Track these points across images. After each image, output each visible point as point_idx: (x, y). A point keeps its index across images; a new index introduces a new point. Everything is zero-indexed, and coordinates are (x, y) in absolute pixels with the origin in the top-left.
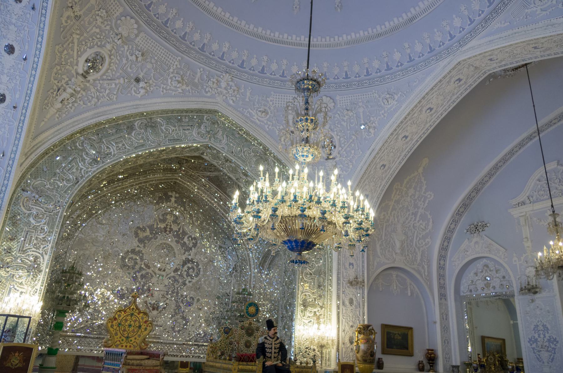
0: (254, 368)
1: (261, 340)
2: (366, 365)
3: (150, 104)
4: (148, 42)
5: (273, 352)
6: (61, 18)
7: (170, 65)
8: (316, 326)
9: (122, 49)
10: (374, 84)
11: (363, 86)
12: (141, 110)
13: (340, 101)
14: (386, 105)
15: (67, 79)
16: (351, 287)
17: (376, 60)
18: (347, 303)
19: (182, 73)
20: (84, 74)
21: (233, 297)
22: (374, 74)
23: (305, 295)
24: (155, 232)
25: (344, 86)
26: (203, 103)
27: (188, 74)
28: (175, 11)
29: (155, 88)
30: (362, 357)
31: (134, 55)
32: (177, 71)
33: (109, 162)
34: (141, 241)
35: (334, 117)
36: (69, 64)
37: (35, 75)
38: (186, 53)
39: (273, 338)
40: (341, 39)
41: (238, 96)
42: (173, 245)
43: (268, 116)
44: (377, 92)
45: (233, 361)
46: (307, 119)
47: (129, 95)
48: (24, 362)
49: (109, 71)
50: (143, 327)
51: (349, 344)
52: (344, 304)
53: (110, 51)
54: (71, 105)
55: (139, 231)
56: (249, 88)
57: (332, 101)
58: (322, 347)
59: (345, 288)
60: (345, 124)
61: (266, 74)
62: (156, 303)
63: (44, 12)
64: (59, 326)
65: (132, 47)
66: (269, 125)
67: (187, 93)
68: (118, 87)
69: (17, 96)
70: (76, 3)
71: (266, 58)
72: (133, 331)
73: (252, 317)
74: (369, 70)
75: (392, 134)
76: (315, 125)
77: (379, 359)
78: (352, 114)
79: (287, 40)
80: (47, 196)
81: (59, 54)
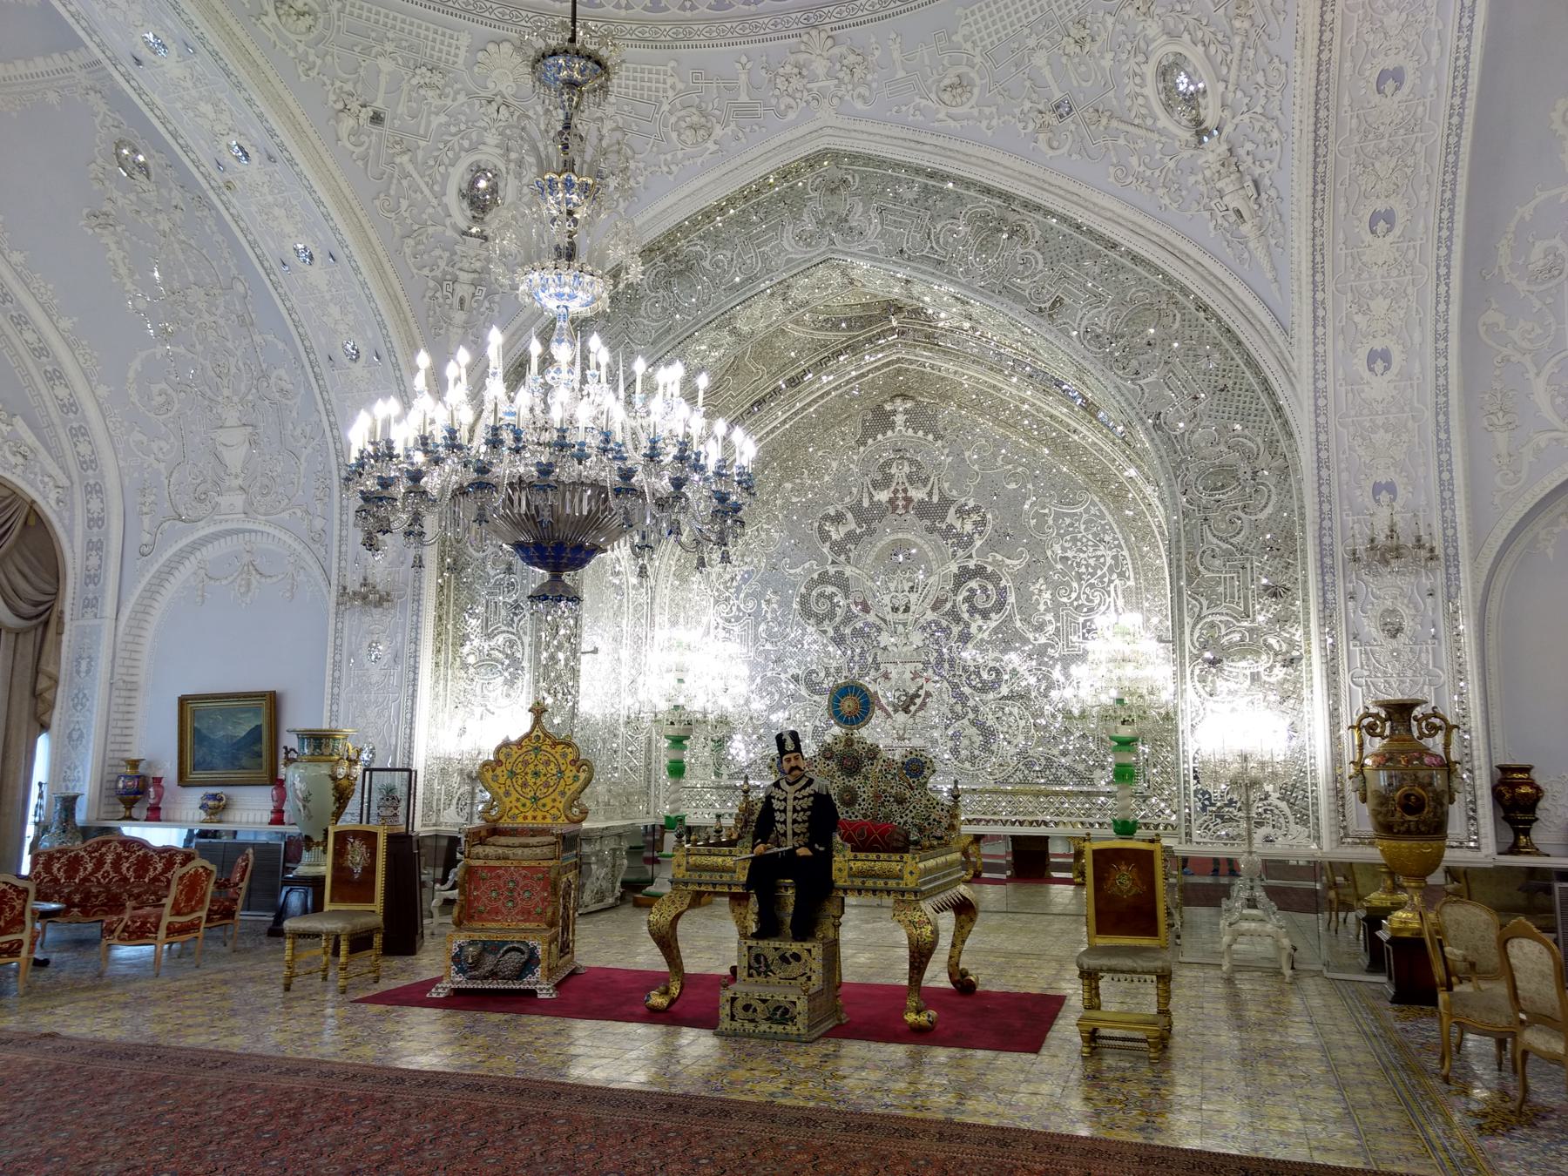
0: (729, 862)
5: (789, 821)
7: (657, 97)
18: (1371, 629)
23: (1212, 625)
24: (868, 517)
34: (839, 548)
36: (429, 223)
38: (681, 40)
43: (976, 91)
54: (487, 304)
55: (828, 527)
56: (893, 36)
66: (991, 117)
69: (370, 335)
72: (547, 785)
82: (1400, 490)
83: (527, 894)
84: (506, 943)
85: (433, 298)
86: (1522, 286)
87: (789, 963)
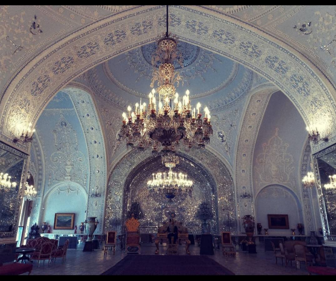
0: (165, 235)
50: (137, 224)
82: (246, 188)
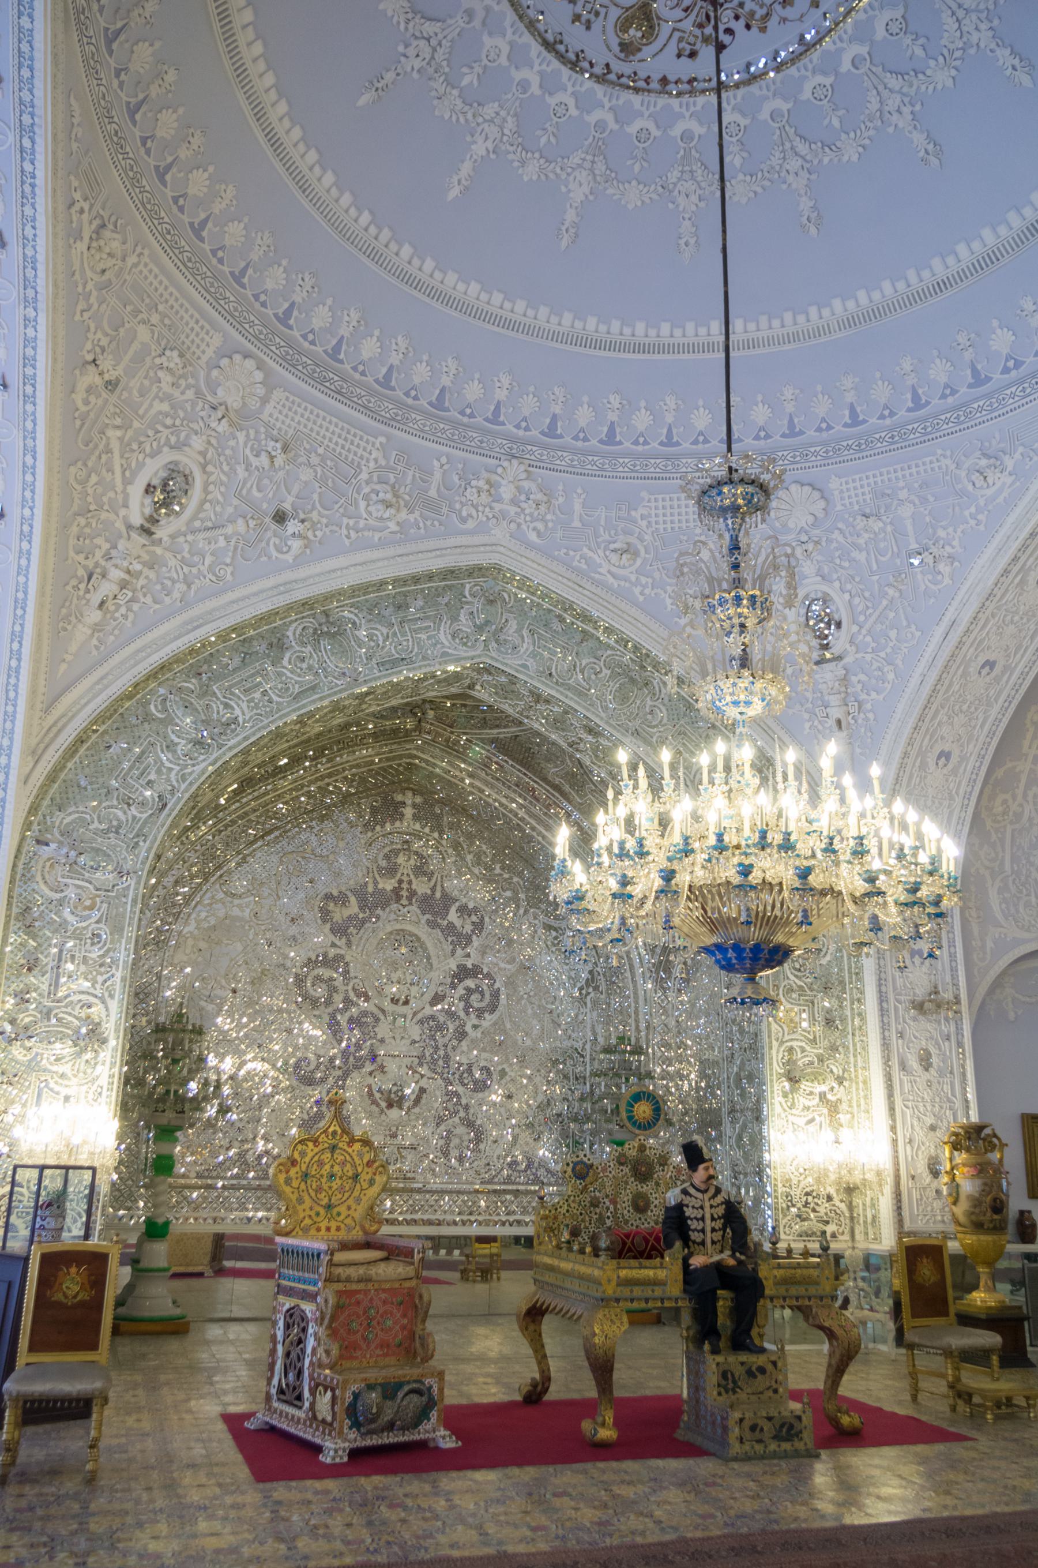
0: (662, 1274)
1: (673, 1197)
2: (983, 1237)
3: (318, 575)
4: (296, 413)
5: (708, 1229)
6: (73, 396)
8: (828, 1134)
9: (232, 443)
10: (938, 430)
11: (905, 440)
12: (301, 594)
13: (842, 491)
14: (981, 488)
15: (106, 546)
16: (921, 1017)
17: (938, 361)
18: (913, 1063)
19: (392, 480)
20: (147, 525)
21: (593, 1059)
22: (935, 401)
23: (791, 1050)
25: (849, 447)
26: (458, 550)
27: (410, 478)
28: (355, 315)
29: (327, 530)
30: (969, 1214)
31: (263, 454)
32: (379, 477)
33: (235, 742)
34: (340, 930)
35: (829, 541)
36: (106, 507)
37: (29, 553)
38: (398, 421)
39: (706, 1191)
40: (826, 312)
41: (549, 517)
42: (422, 931)
43: (639, 562)
44: (948, 453)
45: (603, 1258)
46: (738, 599)
47: (264, 559)
48: (92, 1288)
49: (207, 506)
50: (365, 1177)
51: (927, 1178)
52: (903, 1066)
53: (203, 454)
54: (123, 610)
56: (579, 491)
57: (816, 494)
58: (850, 1190)
59: (904, 1021)
60: (861, 557)
61: (620, 443)
62: (395, 1089)
63: (29, 390)
64: (164, 1165)
65: (257, 432)
66: (645, 587)
67: (412, 531)
68: (233, 543)
70: (103, 350)
71: (618, 400)
72: (342, 1188)
73: (645, 1129)
74: (920, 391)
75: (1006, 572)
76: (762, 609)
77: (1022, 1213)
78: (881, 524)
79: (672, 341)
80: (97, 851)
81: (79, 487)
83: (389, 1323)
84: (400, 1385)
85: (76, 588)
86: (989, 823)
87: (755, 1377)
